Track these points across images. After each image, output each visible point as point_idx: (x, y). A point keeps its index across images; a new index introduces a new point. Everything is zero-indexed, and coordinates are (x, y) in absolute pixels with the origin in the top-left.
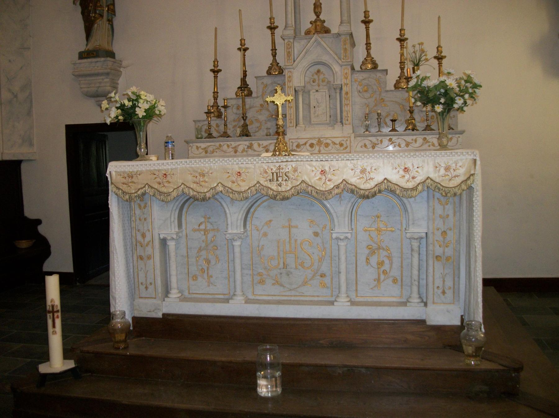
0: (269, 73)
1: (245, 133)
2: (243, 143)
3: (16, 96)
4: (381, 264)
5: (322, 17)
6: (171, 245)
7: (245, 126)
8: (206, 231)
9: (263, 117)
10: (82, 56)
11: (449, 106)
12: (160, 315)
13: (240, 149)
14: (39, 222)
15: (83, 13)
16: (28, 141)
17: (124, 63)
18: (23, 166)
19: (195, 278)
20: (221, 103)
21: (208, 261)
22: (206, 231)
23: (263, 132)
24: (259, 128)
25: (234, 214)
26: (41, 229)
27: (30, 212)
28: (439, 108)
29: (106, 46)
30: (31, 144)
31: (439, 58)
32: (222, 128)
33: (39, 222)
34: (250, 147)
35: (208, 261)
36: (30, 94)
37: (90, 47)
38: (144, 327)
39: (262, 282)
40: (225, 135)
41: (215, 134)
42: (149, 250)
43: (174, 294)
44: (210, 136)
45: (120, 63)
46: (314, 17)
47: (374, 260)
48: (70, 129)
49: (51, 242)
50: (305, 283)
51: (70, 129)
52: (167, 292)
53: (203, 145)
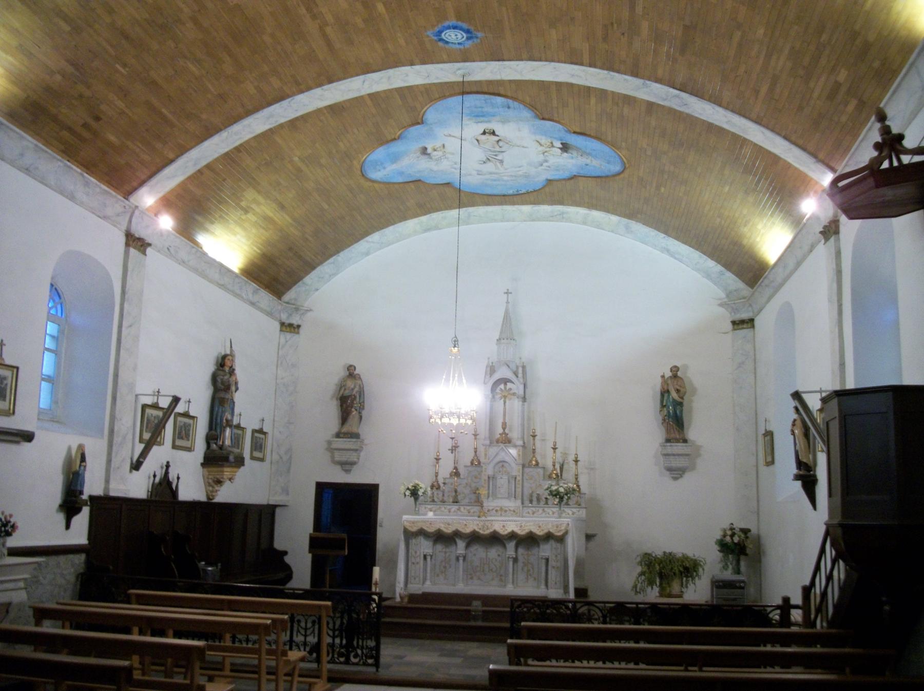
0: (472, 463)
1: (456, 502)
2: (454, 508)
3: (281, 458)
4: (528, 571)
5: (507, 431)
6: (429, 558)
7: (456, 496)
8: (445, 553)
9: (467, 491)
10: (338, 435)
11: (561, 498)
12: (420, 592)
13: (453, 510)
14: (285, 553)
15: (341, 406)
16: (286, 491)
17: (366, 442)
18: (278, 510)
19: (438, 575)
20: (441, 481)
21: (445, 567)
22: (445, 553)
23: (466, 501)
24: (464, 498)
25: (461, 544)
26: (287, 559)
27: (278, 545)
28: (557, 500)
29: (355, 430)
30: (288, 494)
31: (576, 461)
32: (441, 495)
33: (285, 553)
34: (459, 509)
35: (445, 567)
36: (291, 457)
37: (344, 430)
38: (413, 598)
39: (472, 578)
40: (443, 502)
41: (436, 499)
42: (418, 560)
43: (428, 583)
44: (433, 501)
45: (362, 442)
46: (501, 431)
47: (526, 569)
48: (321, 487)
49: (294, 569)
50: (493, 579)
51: (321, 487)
52: (424, 583)
53: (429, 507)
